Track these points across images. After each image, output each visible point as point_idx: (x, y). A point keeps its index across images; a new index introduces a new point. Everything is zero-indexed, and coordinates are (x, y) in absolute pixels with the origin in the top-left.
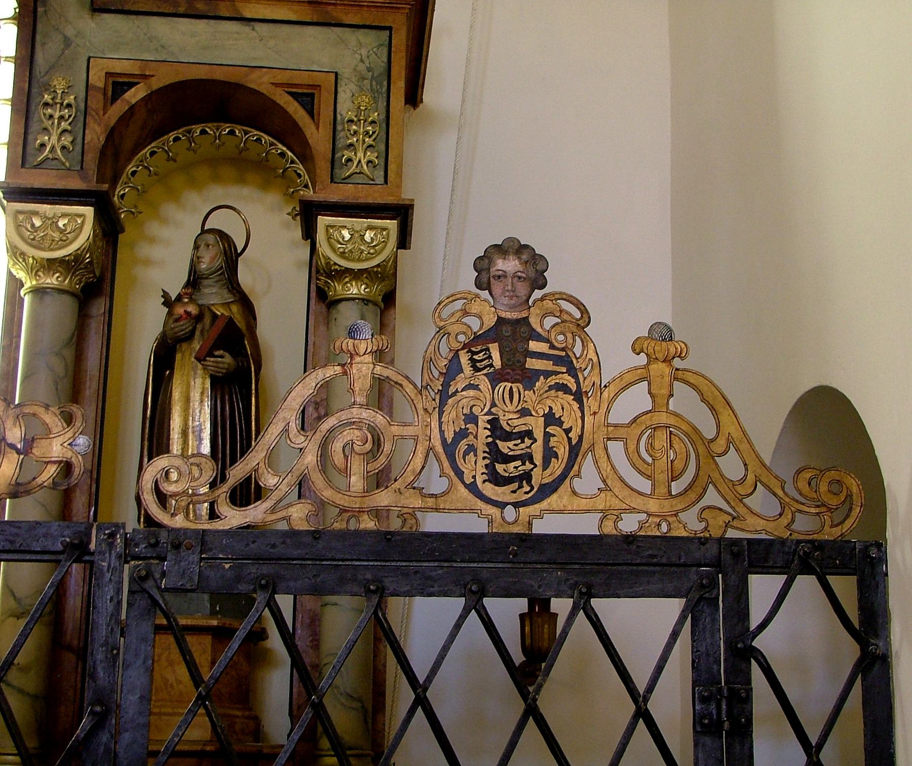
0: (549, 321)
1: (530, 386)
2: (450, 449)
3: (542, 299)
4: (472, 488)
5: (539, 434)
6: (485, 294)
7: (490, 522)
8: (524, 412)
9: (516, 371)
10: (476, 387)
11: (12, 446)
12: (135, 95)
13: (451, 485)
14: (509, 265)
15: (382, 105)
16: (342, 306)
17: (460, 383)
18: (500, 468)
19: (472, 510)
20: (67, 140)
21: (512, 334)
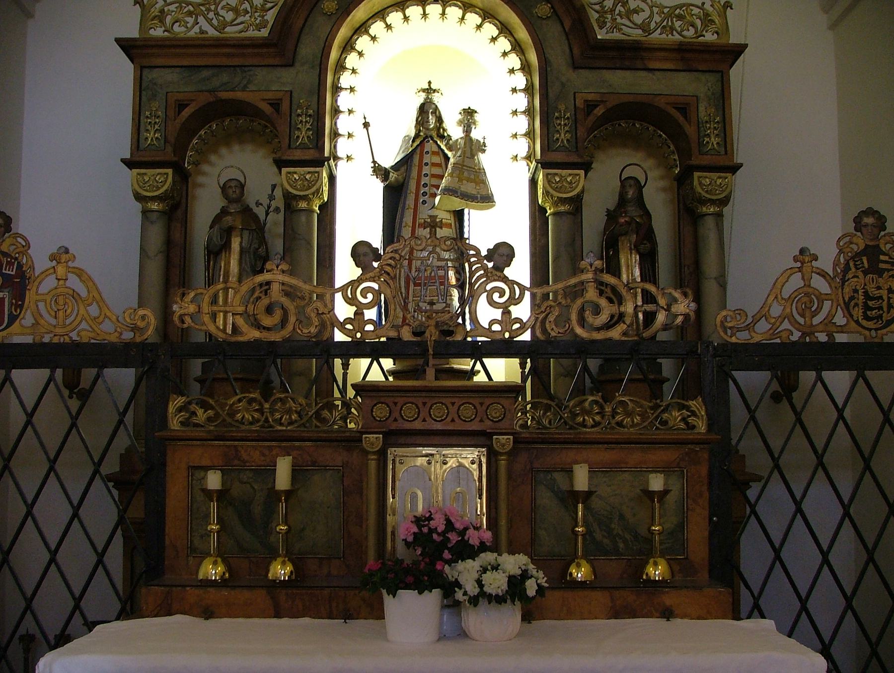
0: (889, 246)
1: (881, 276)
2: (847, 305)
3: (884, 236)
4: (857, 322)
5: (885, 297)
6: (859, 234)
7: (865, 338)
8: (879, 288)
9: (874, 269)
10: (857, 277)
11: (663, 308)
12: (599, 111)
13: (848, 321)
14: (869, 220)
15: (721, 113)
16: (706, 218)
17: (850, 275)
18: (869, 313)
19: (858, 332)
20: (568, 136)
21: (872, 252)
